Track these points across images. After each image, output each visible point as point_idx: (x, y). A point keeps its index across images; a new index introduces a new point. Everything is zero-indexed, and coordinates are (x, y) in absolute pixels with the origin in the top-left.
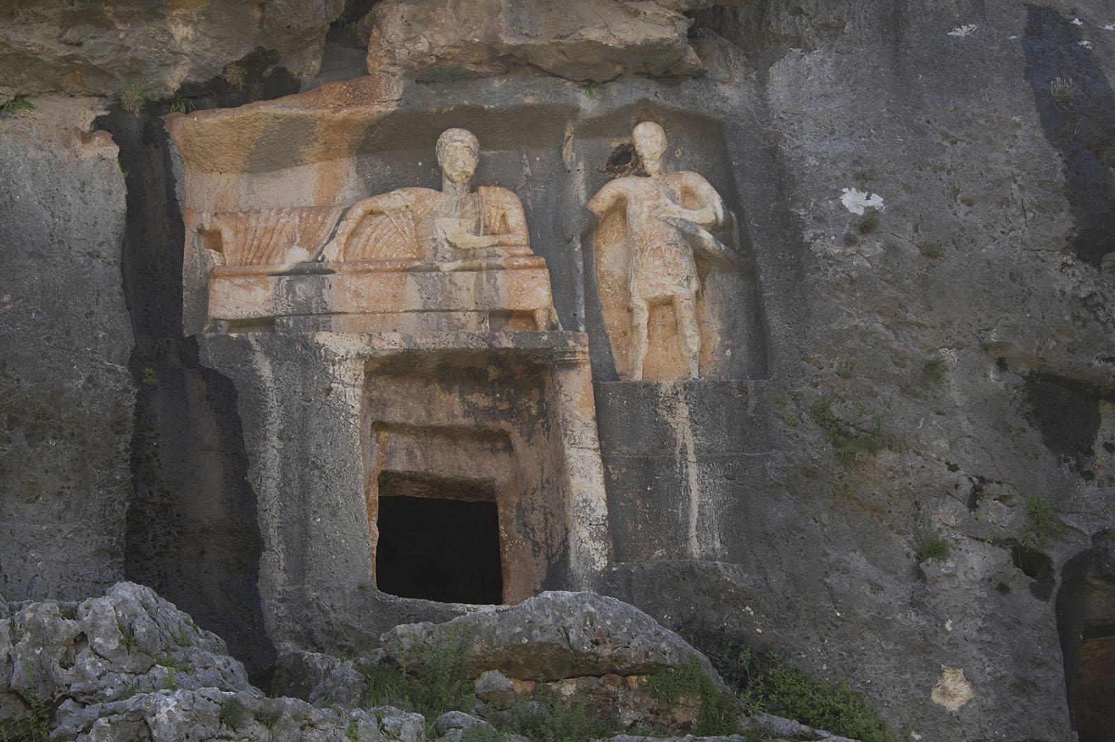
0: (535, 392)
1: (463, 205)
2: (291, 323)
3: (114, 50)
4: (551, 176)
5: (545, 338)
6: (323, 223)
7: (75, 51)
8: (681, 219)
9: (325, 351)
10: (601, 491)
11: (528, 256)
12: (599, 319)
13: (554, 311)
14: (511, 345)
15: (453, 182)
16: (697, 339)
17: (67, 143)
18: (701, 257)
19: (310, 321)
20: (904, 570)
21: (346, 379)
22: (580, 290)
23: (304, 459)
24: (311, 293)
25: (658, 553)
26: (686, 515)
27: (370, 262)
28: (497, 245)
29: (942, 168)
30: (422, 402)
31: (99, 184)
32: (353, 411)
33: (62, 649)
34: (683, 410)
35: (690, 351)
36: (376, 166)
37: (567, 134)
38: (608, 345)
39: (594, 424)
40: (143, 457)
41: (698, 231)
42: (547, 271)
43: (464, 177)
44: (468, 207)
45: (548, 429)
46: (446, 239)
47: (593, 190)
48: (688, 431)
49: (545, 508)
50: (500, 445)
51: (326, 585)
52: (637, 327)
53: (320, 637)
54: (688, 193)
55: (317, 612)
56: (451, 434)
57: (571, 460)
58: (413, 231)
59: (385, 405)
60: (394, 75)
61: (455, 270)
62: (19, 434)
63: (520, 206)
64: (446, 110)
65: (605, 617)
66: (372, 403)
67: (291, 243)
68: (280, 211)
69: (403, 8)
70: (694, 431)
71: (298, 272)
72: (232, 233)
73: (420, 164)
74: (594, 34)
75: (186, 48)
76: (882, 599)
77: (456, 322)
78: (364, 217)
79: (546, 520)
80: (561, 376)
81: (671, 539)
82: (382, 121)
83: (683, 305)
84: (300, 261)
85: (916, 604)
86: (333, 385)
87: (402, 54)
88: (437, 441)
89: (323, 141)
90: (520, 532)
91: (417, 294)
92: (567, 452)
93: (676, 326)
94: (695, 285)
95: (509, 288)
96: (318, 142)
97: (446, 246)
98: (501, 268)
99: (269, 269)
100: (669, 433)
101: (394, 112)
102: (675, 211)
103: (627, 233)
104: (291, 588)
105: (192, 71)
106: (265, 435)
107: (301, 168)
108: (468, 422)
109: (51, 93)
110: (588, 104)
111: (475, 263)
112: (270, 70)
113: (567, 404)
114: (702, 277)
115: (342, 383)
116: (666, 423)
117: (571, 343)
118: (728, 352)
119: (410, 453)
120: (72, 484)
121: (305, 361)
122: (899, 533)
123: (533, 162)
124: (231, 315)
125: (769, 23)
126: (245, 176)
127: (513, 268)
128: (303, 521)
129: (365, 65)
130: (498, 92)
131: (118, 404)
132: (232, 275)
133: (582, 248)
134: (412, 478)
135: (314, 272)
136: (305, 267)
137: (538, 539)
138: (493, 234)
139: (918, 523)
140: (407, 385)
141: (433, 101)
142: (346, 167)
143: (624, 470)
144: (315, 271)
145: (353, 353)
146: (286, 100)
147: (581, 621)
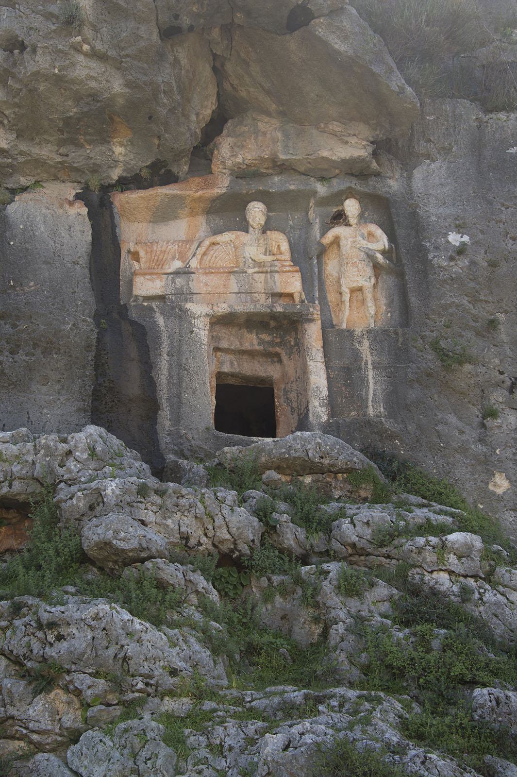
0: (293, 333)
1: (259, 240)
2: (173, 298)
3: (84, 159)
4: (302, 226)
5: (298, 307)
6: (189, 249)
7: (65, 159)
8: (367, 248)
9: (190, 312)
10: (325, 383)
11: (290, 266)
12: (325, 298)
13: (303, 293)
14: (281, 310)
15: (254, 228)
16: (374, 308)
17: (61, 206)
18: (376, 267)
19: (183, 297)
20: (476, 423)
21: (201, 326)
22: (316, 283)
23: (180, 365)
24: (183, 283)
25: (353, 413)
26: (367, 395)
27: (213, 268)
28: (275, 261)
29: (500, 222)
30: (237, 338)
31: (78, 227)
32: (204, 342)
33: (60, 458)
34: (366, 343)
35: (370, 314)
37: (311, 204)
38: (330, 311)
39: (322, 350)
40: (101, 364)
41: (375, 254)
42: (300, 273)
44: (261, 241)
45: (299, 352)
47: (324, 233)
48: (369, 354)
49: (297, 390)
50: (275, 359)
51: (190, 427)
52: (344, 301)
53: (187, 453)
54: (371, 234)
55: (185, 440)
56: (251, 354)
57: (311, 367)
59: (220, 340)
60: (225, 174)
61: (254, 273)
62: (39, 351)
63: (287, 240)
64: (251, 192)
65: (327, 445)
66: (213, 338)
67: (174, 258)
68: (168, 242)
69: (230, 139)
70: (371, 353)
71: (177, 273)
72: (144, 253)
74: (325, 154)
75: (121, 158)
76: (464, 437)
77: (255, 299)
78: (210, 245)
79: (298, 396)
80: (306, 326)
81: (359, 406)
82: (219, 197)
83: (367, 291)
84: (178, 267)
85: (481, 440)
86: (194, 329)
87: (229, 163)
88: (245, 357)
90: (285, 402)
91: (235, 285)
92: (308, 363)
93: (363, 302)
94: (373, 281)
95: (281, 282)
97: (250, 260)
98: (278, 272)
99: (163, 271)
100: (359, 355)
101: (225, 193)
102: (364, 244)
103: (340, 255)
104: (173, 429)
105: (124, 170)
106: (160, 354)
107: (177, 221)
108: (260, 348)
109: (53, 180)
110: (322, 189)
111: (265, 269)
112: (163, 171)
113: (309, 340)
114: (377, 278)
115: (199, 328)
116: (358, 349)
117: (311, 309)
118: (389, 315)
119: (232, 363)
120: (65, 376)
121: (180, 317)
122: (473, 405)
123: (294, 219)
124: (144, 294)
125: (414, 147)
126: (151, 224)
127: (283, 272)
128: (179, 396)
129: (211, 168)
130: (277, 183)
131: (88, 337)
132: (144, 274)
133: (317, 262)
134: (233, 375)
135: (185, 273)
136: (180, 270)
137: (293, 406)
138: (274, 255)
139: (483, 400)
140: (230, 330)
141: (245, 187)
142: (201, 220)
143: (336, 373)
144: (185, 272)
145: (204, 314)
146: (171, 186)
147: (315, 446)
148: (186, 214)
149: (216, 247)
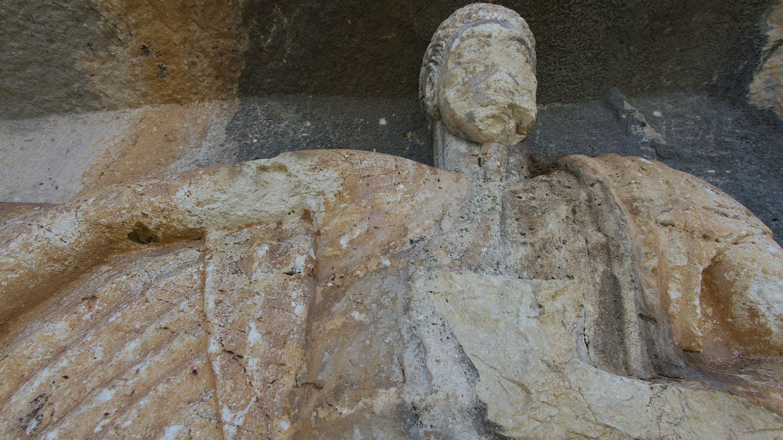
1: (529, 218)
15: (473, 141)
36: (280, 120)
43: (512, 124)
46: (480, 410)
58: (291, 355)
73: (383, 122)
89: (135, 44)
96: (122, 43)
107: (92, 116)
148: (128, 84)
149: (147, 270)
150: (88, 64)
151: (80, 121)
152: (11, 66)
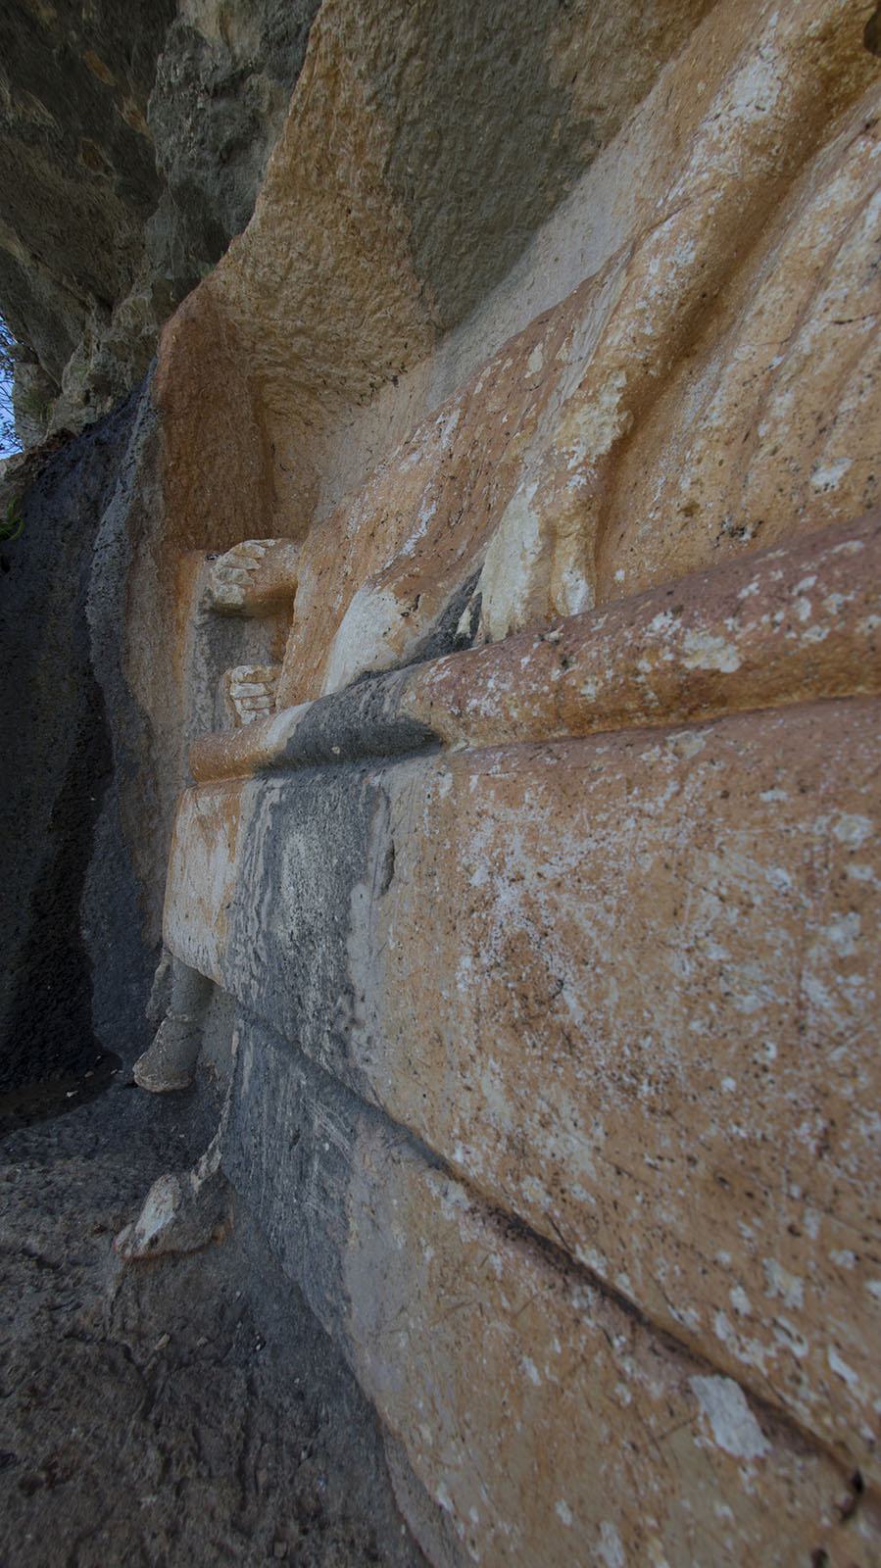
107: (587, 180)
150: (564, 56)
151: (575, 204)
152: (483, 171)
